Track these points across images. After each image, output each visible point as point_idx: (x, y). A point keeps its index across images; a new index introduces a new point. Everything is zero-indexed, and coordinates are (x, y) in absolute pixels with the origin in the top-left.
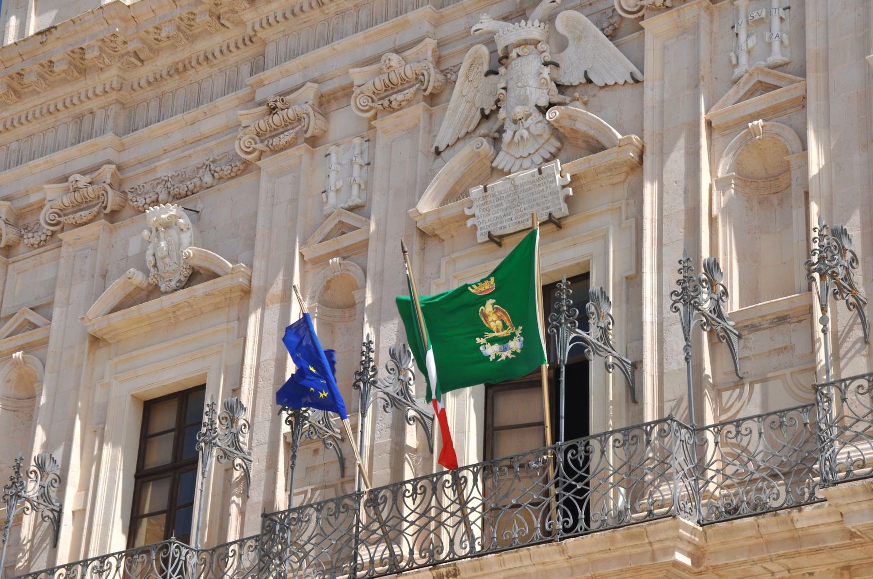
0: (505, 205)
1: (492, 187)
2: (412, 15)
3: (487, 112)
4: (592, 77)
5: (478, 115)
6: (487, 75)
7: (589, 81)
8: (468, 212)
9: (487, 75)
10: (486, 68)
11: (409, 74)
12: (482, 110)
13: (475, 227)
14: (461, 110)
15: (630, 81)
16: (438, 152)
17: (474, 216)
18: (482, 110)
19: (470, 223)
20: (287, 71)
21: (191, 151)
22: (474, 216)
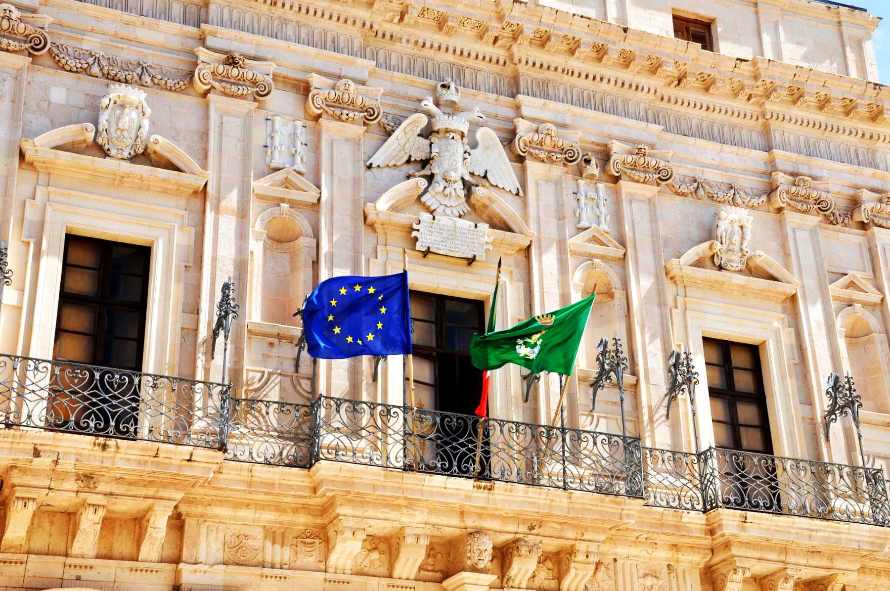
0: (444, 235)
1: (439, 220)
2: (360, 61)
3: (413, 159)
4: (488, 176)
5: (406, 158)
6: (419, 135)
7: (485, 177)
8: (415, 226)
9: (419, 135)
10: (418, 132)
11: (359, 102)
12: (410, 156)
13: (416, 239)
14: (394, 147)
15: (515, 192)
16: (370, 167)
17: (418, 230)
18: (410, 156)
19: (414, 234)
20: (241, 38)
21: (125, 46)
22: (418, 230)
